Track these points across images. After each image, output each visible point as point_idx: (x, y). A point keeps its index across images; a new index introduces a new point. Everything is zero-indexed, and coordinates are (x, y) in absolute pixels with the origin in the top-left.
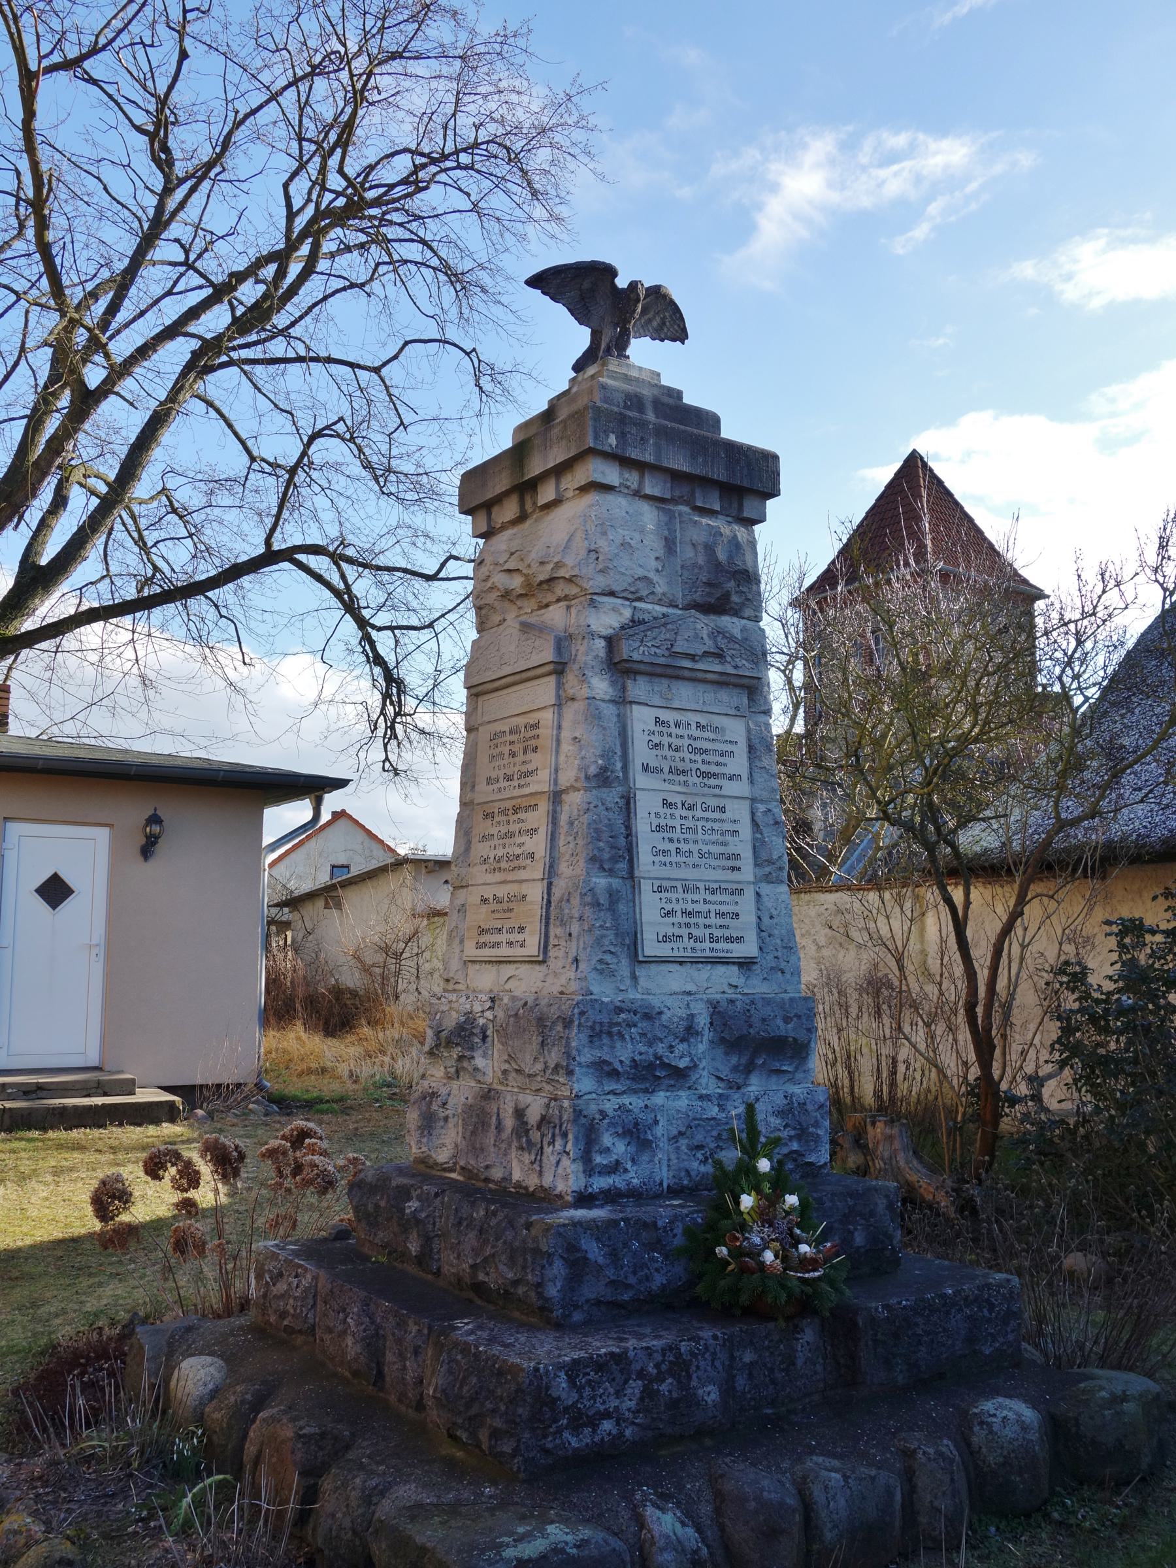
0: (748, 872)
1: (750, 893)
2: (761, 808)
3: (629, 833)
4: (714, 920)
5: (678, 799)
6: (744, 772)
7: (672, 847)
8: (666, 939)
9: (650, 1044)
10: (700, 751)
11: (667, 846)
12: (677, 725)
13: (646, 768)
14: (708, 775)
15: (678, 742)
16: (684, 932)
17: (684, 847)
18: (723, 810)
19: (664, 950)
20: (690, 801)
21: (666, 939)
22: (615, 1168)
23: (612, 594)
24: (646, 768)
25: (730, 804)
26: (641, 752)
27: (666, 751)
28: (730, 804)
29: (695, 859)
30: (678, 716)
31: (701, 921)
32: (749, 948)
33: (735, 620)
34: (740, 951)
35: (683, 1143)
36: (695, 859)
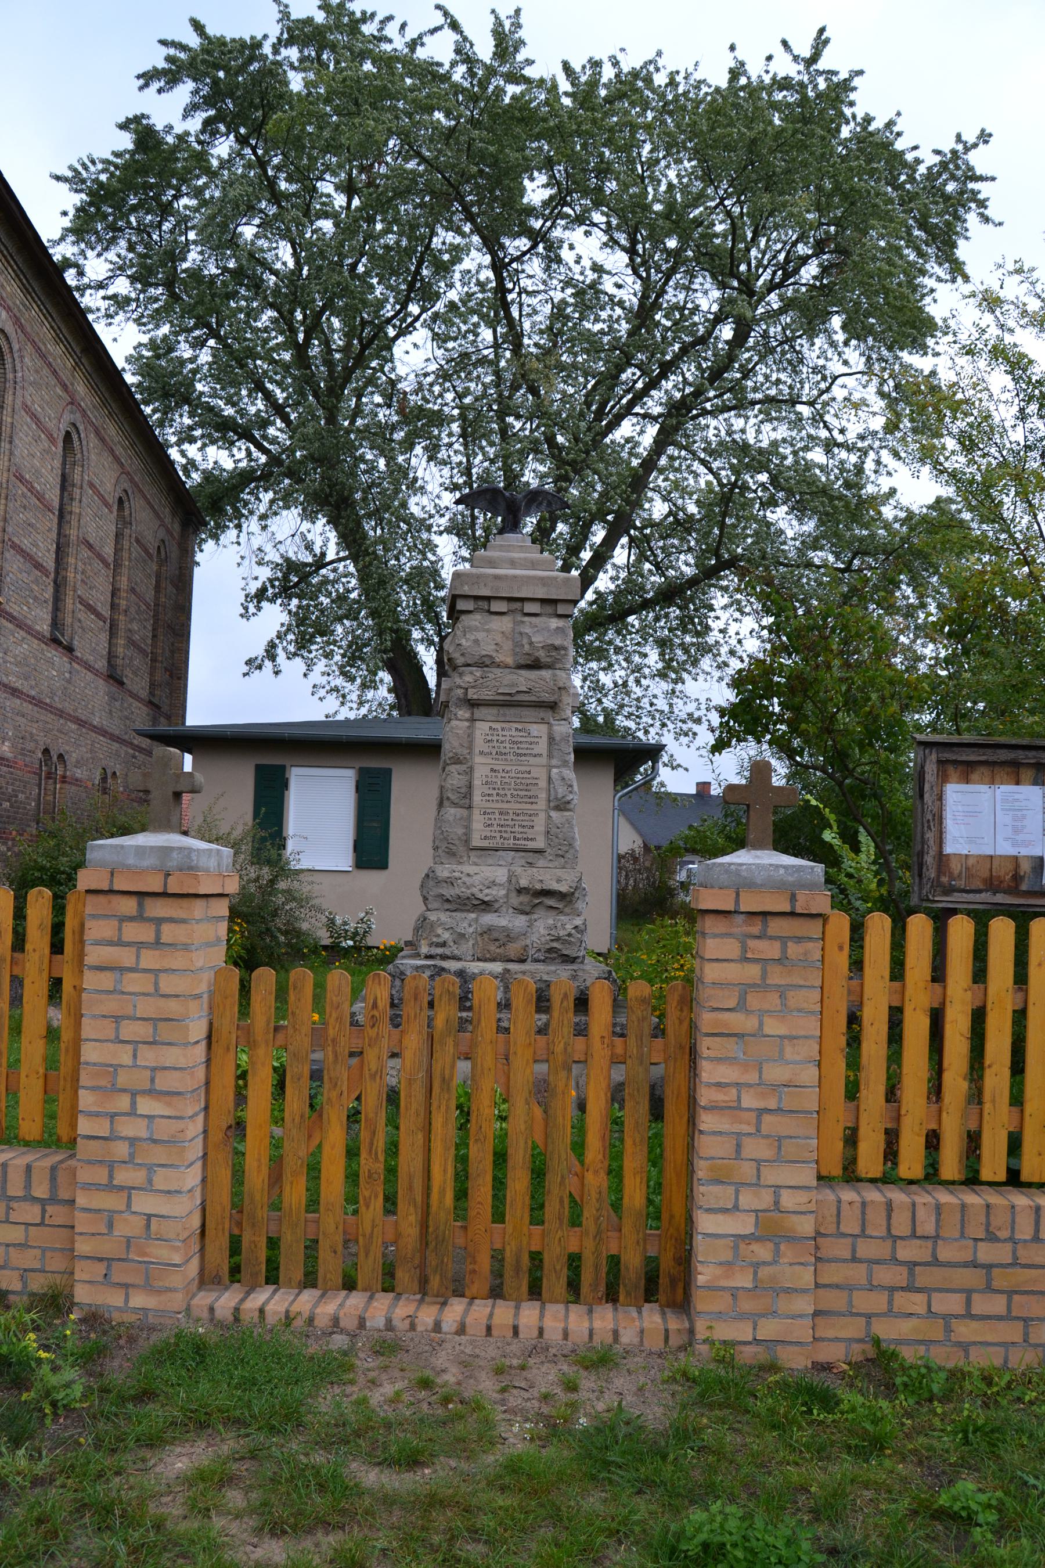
0: (542, 804)
1: (542, 816)
2: (555, 771)
3: (470, 786)
4: (517, 829)
5: (500, 768)
6: (545, 753)
7: (494, 792)
8: (486, 838)
9: (468, 888)
10: (516, 743)
11: (491, 792)
12: (503, 729)
13: (481, 753)
14: (521, 755)
15: (501, 739)
16: (498, 835)
17: (501, 792)
18: (529, 772)
19: (485, 844)
20: (508, 768)
21: (486, 838)
22: (444, 944)
23: (469, 665)
24: (481, 753)
25: (533, 770)
26: (479, 744)
27: (495, 744)
28: (533, 770)
29: (509, 798)
30: (504, 725)
31: (509, 829)
32: (540, 843)
33: (550, 672)
34: (531, 845)
35: (486, 936)
36: (509, 798)
